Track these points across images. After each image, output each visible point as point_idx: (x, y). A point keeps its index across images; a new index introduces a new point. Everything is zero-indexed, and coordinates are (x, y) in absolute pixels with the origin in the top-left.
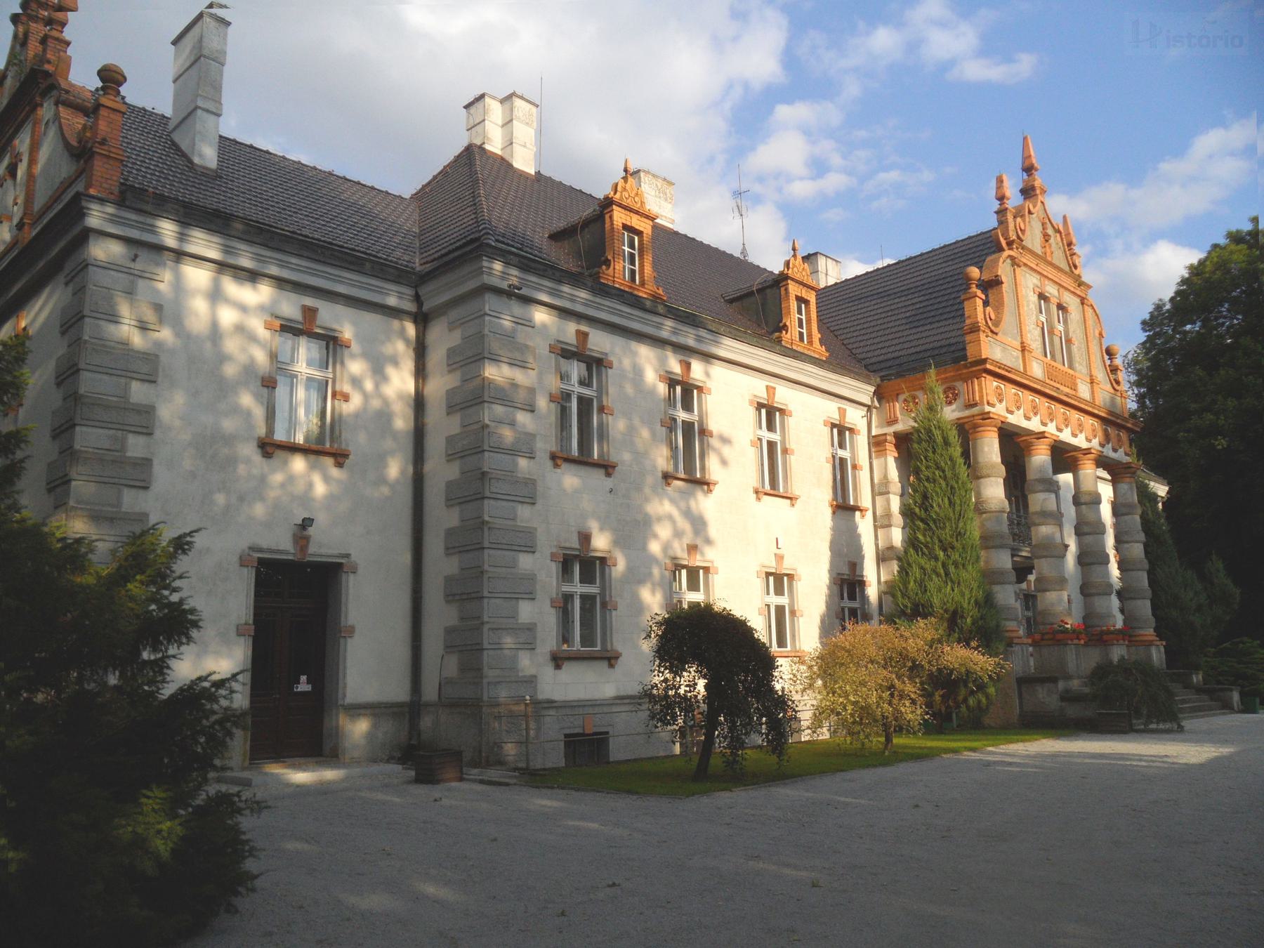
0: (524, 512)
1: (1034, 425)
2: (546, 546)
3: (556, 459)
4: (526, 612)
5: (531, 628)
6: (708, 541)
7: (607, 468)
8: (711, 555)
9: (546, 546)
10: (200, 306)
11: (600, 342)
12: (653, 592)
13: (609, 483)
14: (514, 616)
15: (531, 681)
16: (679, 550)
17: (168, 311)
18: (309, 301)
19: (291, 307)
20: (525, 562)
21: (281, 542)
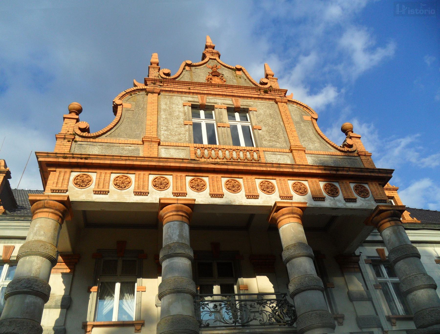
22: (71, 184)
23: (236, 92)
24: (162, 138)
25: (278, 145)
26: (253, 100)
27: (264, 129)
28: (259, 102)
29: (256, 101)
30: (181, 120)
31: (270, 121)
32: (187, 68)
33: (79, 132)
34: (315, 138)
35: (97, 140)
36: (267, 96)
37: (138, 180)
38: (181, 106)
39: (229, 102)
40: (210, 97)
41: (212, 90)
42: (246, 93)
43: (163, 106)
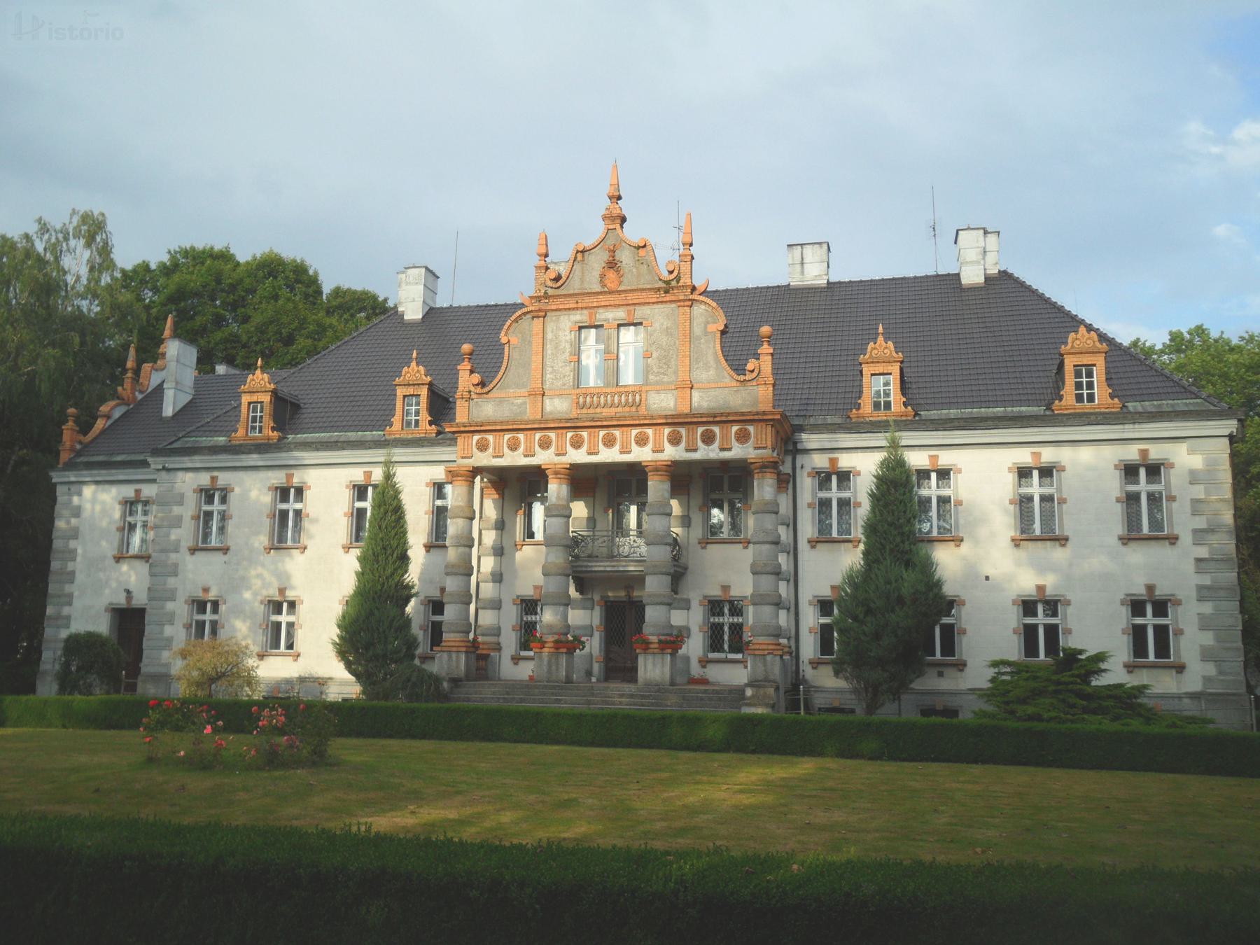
0: (171, 582)
1: (542, 458)
2: (182, 596)
3: (193, 551)
4: (168, 631)
5: (170, 640)
6: (293, 588)
7: (225, 550)
8: (290, 595)
9: (182, 596)
10: (88, 506)
11: (224, 478)
12: (244, 621)
13: (226, 558)
14: (162, 632)
15: (168, 665)
16: (273, 593)
17: (77, 512)
18: (138, 486)
19: (129, 491)
20: (170, 606)
21: (121, 600)
22: (475, 449)
23: (632, 298)
24: (547, 386)
25: (666, 379)
26: (651, 306)
27: (654, 355)
28: (658, 308)
29: (656, 306)
30: (567, 354)
31: (664, 340)
32: (579, 255)
33: (472, 389)
34: (712, 363)
35: (490, 395)
36: (669, 297)
37: (526, 439)
38: (567, 333)
39: (621, 314)
40: (601, 310)
41: (603, 300)
42: (643, 297)
43: (549, 336)
